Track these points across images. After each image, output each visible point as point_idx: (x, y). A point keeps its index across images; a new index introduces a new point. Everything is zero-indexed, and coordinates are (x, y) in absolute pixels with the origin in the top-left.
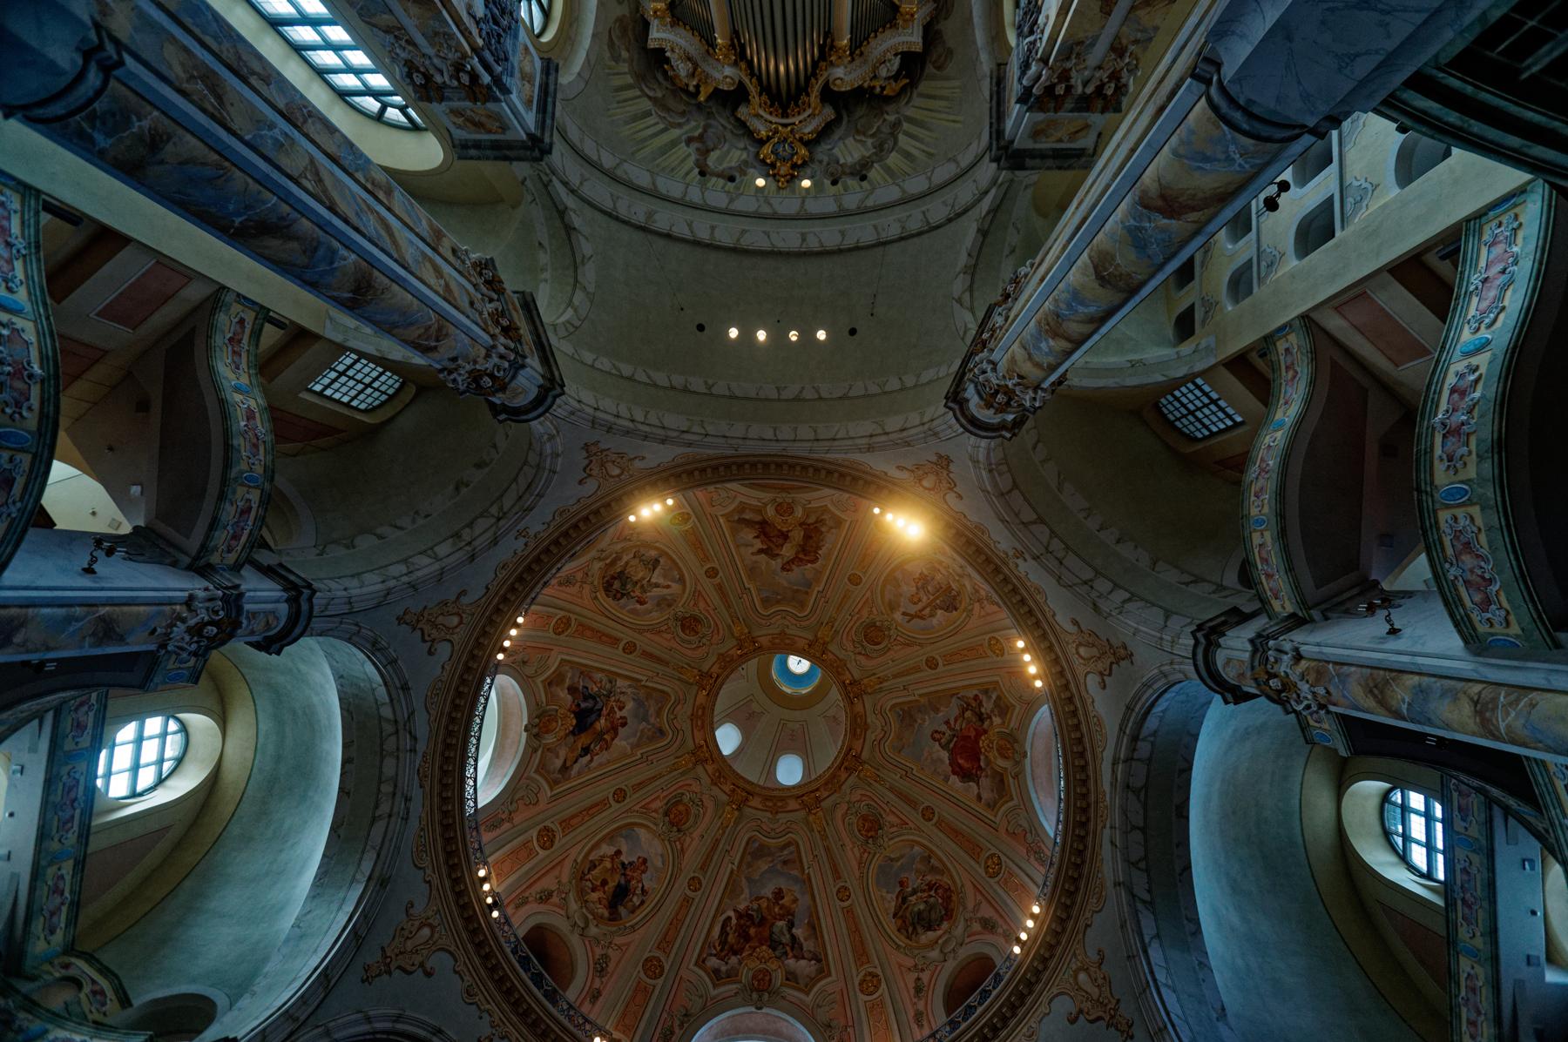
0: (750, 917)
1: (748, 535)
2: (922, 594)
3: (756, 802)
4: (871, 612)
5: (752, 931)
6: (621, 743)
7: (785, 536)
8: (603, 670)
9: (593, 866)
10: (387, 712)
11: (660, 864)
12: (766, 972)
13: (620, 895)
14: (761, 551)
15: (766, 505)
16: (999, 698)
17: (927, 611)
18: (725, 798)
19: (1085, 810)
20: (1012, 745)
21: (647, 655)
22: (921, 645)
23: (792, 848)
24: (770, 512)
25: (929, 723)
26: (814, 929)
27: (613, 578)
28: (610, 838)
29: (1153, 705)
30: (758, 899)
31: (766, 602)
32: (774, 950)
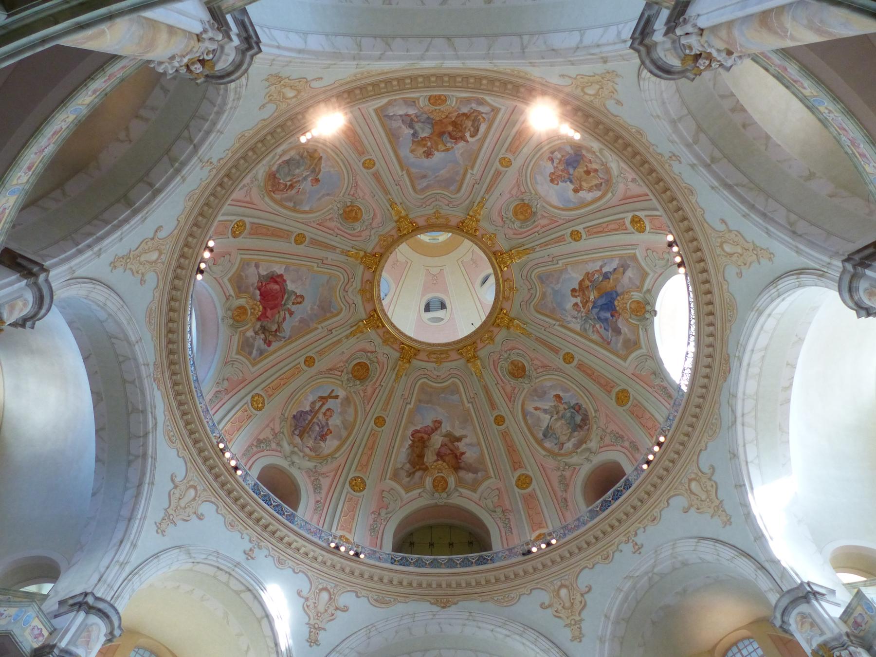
0: (452, 137)
1: (470, 455)
3: (454, 222)
4: (365, 391)
5: (450, 128)
6: (575, 277)
9: (598, 187)
10: (750, 434)
11: (539, 178)
14: (459, 439)
16: (250, 353)
17: (318, 405)
19: (172, 363)
21: (556, 350)
22: (321, 373)
23: (419, 187)
24: (452, 481)
26: (393, 137)
27: (581, 427)
28: (583, 204)
30: (448, 150)
31: (454, 390)
32: (428, 118)
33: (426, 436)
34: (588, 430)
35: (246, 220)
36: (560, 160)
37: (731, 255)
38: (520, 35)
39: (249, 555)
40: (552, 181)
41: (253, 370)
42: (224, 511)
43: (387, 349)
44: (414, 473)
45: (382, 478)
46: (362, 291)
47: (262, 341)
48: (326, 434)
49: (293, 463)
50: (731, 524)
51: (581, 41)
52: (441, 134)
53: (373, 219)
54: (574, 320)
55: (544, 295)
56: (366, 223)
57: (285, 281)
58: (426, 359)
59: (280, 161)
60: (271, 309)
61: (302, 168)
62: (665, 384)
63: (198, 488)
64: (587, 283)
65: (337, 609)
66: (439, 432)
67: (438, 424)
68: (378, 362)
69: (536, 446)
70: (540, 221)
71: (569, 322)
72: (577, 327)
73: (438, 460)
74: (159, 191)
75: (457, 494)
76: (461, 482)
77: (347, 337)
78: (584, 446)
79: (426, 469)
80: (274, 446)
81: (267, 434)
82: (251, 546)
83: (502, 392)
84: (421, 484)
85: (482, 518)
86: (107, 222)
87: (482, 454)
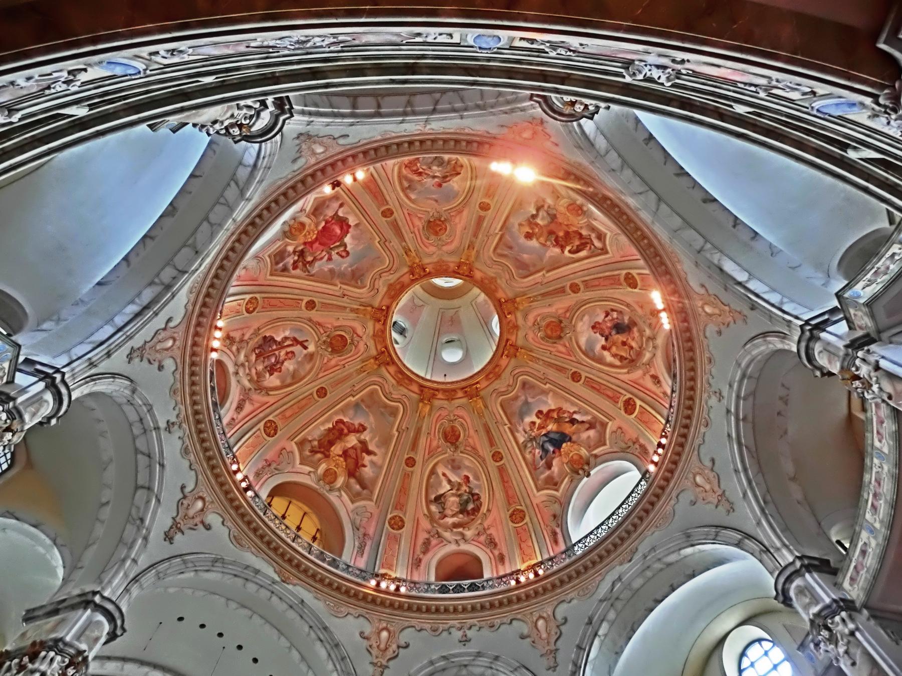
0: (556, 240)
1: (367, 472)
3: (500, 295)
5: (561, 234)
6: (551, 403)
8: (524, 458)
9: (622, 358)
11: (586, 318)
13: (620, 328)
14: (369, 453)
15: (339, 490)
16: (277, 263)
22: (310, 320)
24: (340, 481)
27: (468, 514)
28: (600, 360)
29: (137, 315)
30: (544, 245)
31: (394, 412)
33: (346, 431)
34: (473, 520)
36: (613, 319)
37: (698, 485)
38: (706, 241)
39: (169, 425)
40: (593, 327)
41: (269, 277)
43: (371, 343)
44: (317, 452)
45: (291, 438)
46: (390, 286)
47: (292, 261)
48: (276, 370)
49: (237, 373)
50: (554, 671)
51: (747, 281)
53: (447, 244)
55: (516, 398)
57: (348, 232)
58: (393, 373)
60: (320, 244)
62: (558, 530)
66: (358, 435)
67: (362, 429)
68: (356, 347)
71: (518, 431)
72: (521, 440)
73: (340, 456)
75: (337, 493)
76: (347, 487)
77: (352, 310)
78: (461, 530)
79: (327, 456)
80: (234, 348)
84: (316, 466)
87: (377, 477)
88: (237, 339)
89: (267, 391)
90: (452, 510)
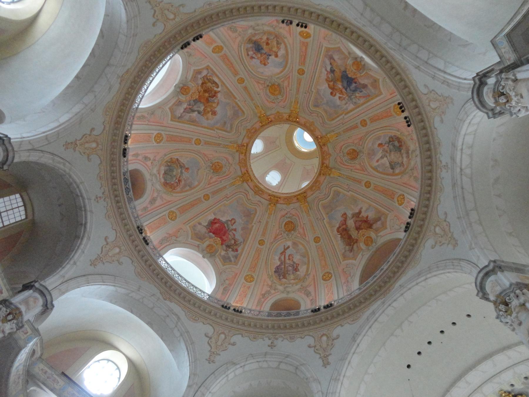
1: (372, 215)
2: (292, 263)
3: (258, 125)
5: (207, 95)
6: (324, 87)
7: (358, 229)
8: (363, 104)
9: (278, 43)
12: (187, 94)
13: (258, 48)
14: (360, 212)
15: (377, 237)
16: (231, 261)
17: (283, 258)
18: (268, 114)
20: (209, 253)
22: (272, 243)
23: (229, 129)
24: (373, 235)
25: (240, 222)
26: (192, 122)
27: (401, 146)
28: (286, 57)
29: (188, 354)
31: (337, 194)
32: (194, 101)
33: (344, 226)
35: (172, 209)
36: (254, 53)
39: (272, 346)
42: (246, 334)
43: (292, 206)
44: (353, 248)
46: (256, 193)
47: (232, 253)
49: (288, 292)
52: (207, 101)
54: (347, 105)
56: (227, 165)
57: (219, 219)
59: (161, 176)
60: (224, 235)
61: (175, 170)
63: (225, 332)
64: (331, 83)
65: (333, 340)
66: (348, 219)
68: (293, 215)
69: (394, 177)
70: (285, 85)
71: (347, 109)
73: (359, 232)
74: (86, 224)
75: (379, 238)
78: (410, 152)
79: (357, 241)
80: (273, 292)
81: (266, 289)
82: (270, 341)
83: (358, 171)
84: (359, 249)
85: (395, 237)
86: (73, 251)
88: (269, 289)
89: (307, 274)
90: (399, 157)
